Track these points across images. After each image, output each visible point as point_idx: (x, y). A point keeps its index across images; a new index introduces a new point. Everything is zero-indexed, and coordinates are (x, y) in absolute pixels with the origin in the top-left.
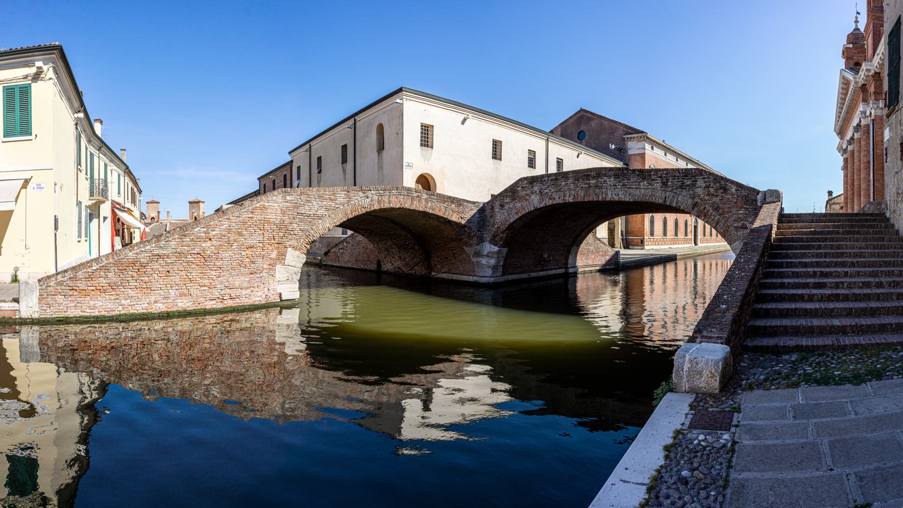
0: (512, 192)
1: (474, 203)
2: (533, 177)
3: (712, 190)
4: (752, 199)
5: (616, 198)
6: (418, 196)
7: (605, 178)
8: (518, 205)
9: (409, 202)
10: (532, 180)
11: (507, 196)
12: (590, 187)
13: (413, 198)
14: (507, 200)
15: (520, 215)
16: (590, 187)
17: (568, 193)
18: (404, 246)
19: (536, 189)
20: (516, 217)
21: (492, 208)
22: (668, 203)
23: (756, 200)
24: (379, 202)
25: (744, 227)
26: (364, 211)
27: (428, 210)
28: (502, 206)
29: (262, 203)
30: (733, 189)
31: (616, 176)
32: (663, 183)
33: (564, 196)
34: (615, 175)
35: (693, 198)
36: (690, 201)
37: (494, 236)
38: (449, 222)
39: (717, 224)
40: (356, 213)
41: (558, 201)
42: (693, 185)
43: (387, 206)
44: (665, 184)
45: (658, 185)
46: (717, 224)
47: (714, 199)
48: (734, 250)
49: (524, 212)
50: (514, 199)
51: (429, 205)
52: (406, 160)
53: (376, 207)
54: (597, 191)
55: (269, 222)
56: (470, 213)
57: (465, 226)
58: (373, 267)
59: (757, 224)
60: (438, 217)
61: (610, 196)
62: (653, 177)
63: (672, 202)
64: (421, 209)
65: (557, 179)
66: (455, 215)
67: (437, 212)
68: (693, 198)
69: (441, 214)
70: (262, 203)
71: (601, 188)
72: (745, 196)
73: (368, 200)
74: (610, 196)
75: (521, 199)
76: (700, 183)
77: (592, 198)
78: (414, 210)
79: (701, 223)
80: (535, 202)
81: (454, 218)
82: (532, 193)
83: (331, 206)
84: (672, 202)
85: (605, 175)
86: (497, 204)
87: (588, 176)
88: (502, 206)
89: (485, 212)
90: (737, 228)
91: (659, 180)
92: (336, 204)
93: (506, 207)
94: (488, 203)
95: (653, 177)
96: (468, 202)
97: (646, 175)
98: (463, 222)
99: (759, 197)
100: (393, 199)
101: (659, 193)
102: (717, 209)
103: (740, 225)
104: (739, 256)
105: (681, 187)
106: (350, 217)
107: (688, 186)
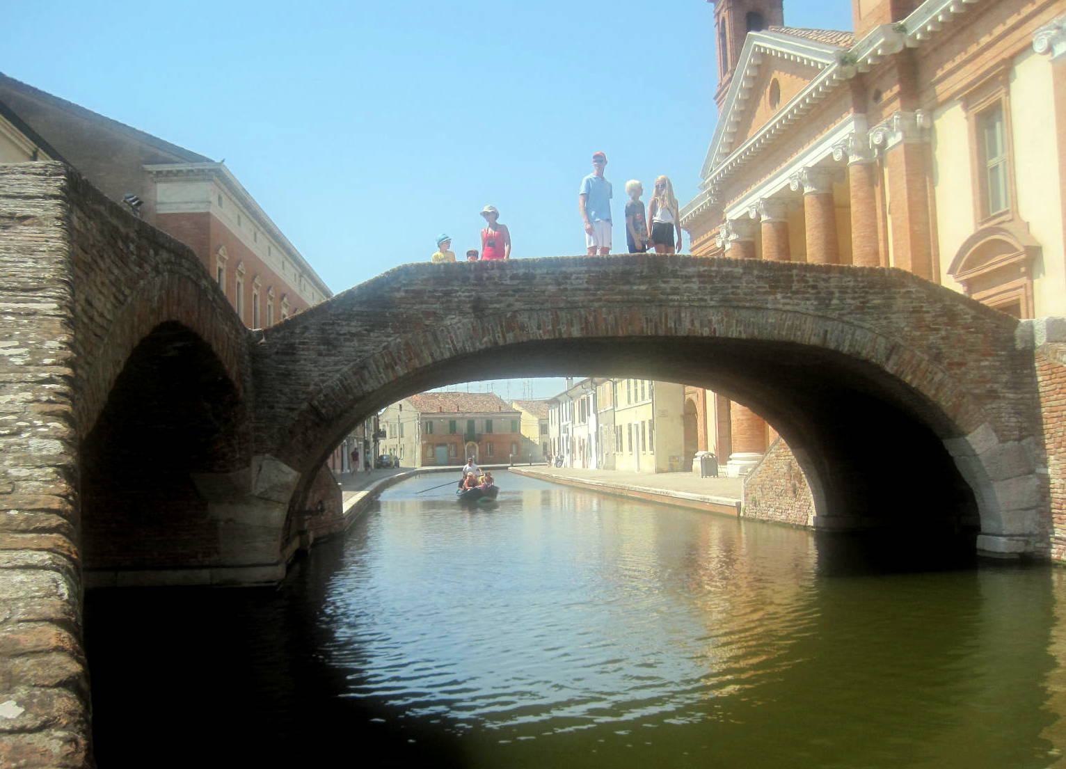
5: (706, 332)
7: (673, 283)
17: (563, 315)
33: (556, 321)
36: (881, 340)
76: (899, 303)
95: (795, 286)
107: (875, 307)
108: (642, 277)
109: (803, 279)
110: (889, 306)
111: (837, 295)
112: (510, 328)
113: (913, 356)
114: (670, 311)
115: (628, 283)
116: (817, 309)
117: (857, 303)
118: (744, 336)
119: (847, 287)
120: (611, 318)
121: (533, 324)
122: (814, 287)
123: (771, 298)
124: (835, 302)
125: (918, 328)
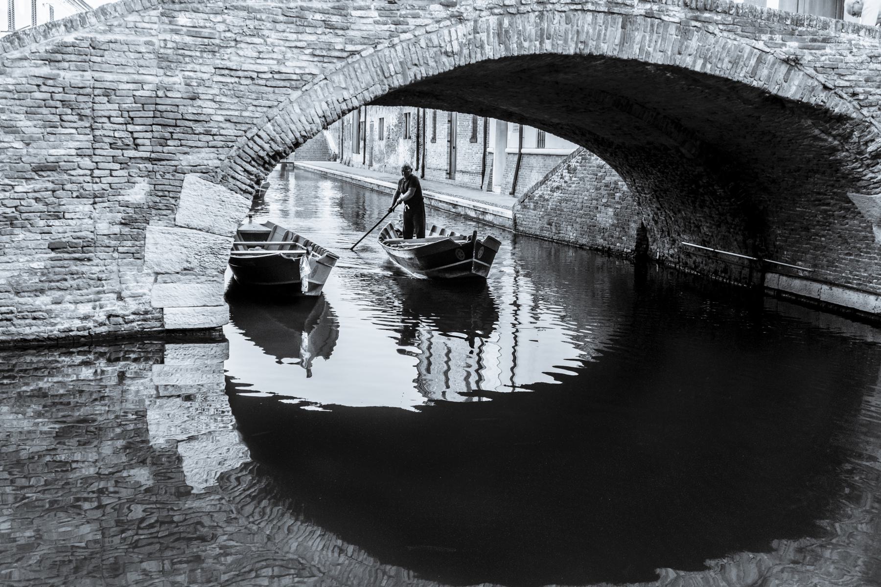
6: (649, 15)
9: (615, 33)
13: (627, 19)
24: (502, 35)
26: (448, 64)
27: (686, 62)
29: (81, 33)
40: (422, 72)
43: (532, 47)
51: (694, 43)
53: (493, 51)
55: (108, 93)
58: (628, 245)
64: (658, 59)
67: (722, 68)
69: (740, 75)
70: (81, 33)
73: (462, 30)
78: (635, 61)
83: (330, 47)
92: (351, 41)
100: (557, 24)
106: (398, 82)
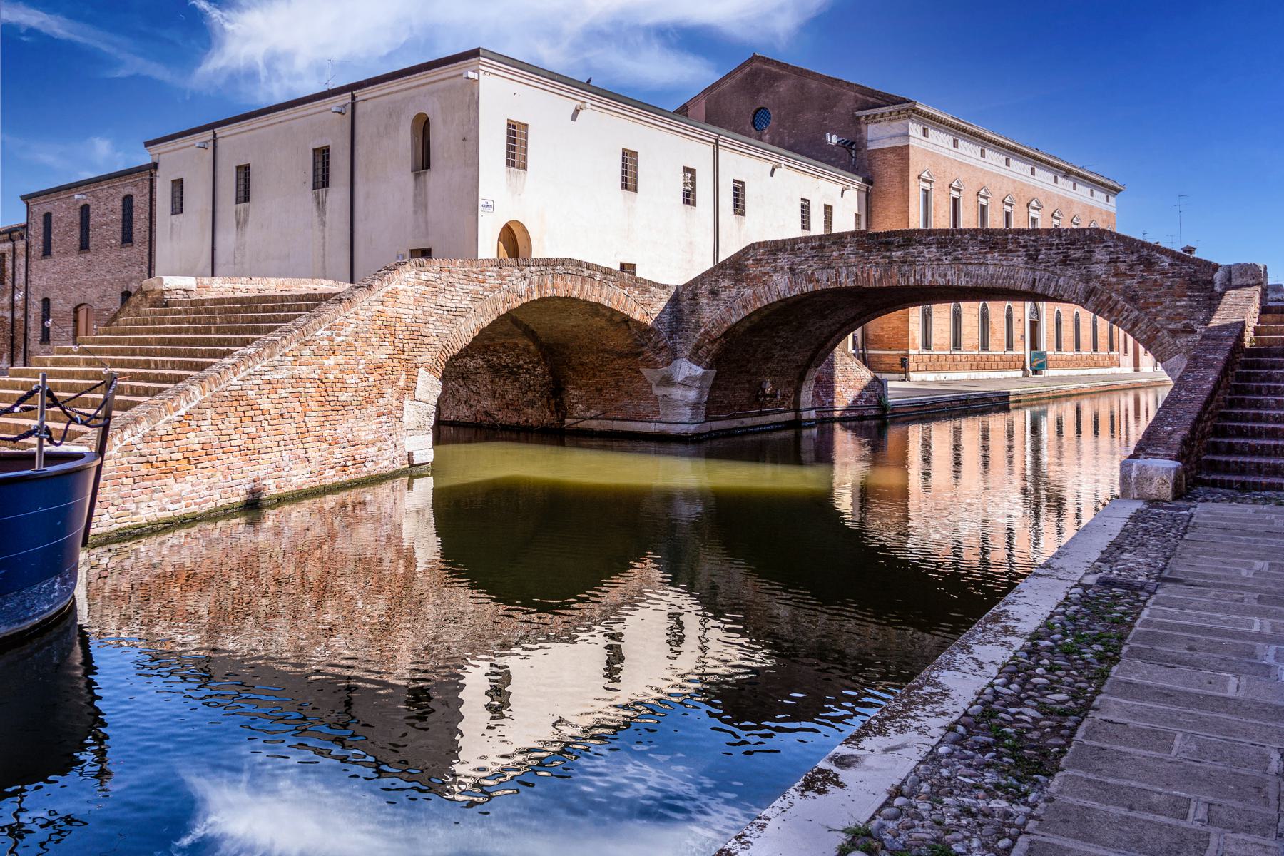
0: (734, 268)
1: (664, 286)
2: (776, 242)
3: (1122, 267)
4: (1202, 282)
5: (942, 282)
7: (920, 248)
8: (748, 292)
10: (775, 248)
11: (725, 276)
12: (892, 262)
14: (726, 283)
15: (751, 309)
16: (892, 262)
17: (844, 272)
18: (544, 363)
19: (783, 262)
20: (744, 313)
21: (695, 298)
22: (1039, 291)
23: (1212, 282)
25: (1189, 330)
28: (714, 293)
30: (1166, 262)
31: (941, 244)
32: (1030, 257)
33: (838, 276)
34: (939, 242)
35: (1087, 280)
36: (1081, 286)
37: (697, 348)
38: (627, 320)
39: (1134, 325)
41: (824, 284)
42: (1087, 258)
44: (1033, 258)
45: (1019, 259)
46: (1134, 325)
47: (1128, 282)
48: (1169, 371)
49: (759, 305)
50: (738, 280)
52: (483, 194)
54: (906, 269)
56: (659, 304)
57: (651, 330)
59: (1216, 322)
60: (614, 312)
61: (929, 277)
62: (1010, 247)
63: (1046, 287)
65: (822, 247)
66: (639, 309)
68: (1087, 281)
71: (912, 264)
72: (1191, 276)
74: (929, 277)
75: (753, 281)
76: (1100, 254)
77: (896, 280)
79: (1103, 324)
80: (781, 286)
81: (637, 317)
82: (775, 271)
84: (1046, 287)
85: (920, 242)
86: (705, 290)
87: (888, 243)
88: (714, 293)
89: (682, 302)
90: (1174, 333)
91: (1022, 252)
93: (724, 295)
94: (684, 287)
95: (1010, 247)
96: (656, 285)
97: (992, 240)
98: (650, 322)
99: (1218, 276)
101: (1022, 274)
102: (1133, 299)
103: (1179, 326)
104: (1180, 382)
105: (1065, 262)
107: (1078, 260)
108: (898, 246)
109: (1016, 241)
110: (1089, 259)
111: (1043, 251)
112: (811, 282)
113: (1110, 298)
114: (918, 268)
115: (889, 250)
116: (1027, 263)
117: (1061, 256)
118: (970, 285)
119: (1052, 245)
120: (878, 275)
121: (824, 278)
122: (1024, 246)
123: (989, 256)
124: (1041, 257)
125: (1115, 275)
